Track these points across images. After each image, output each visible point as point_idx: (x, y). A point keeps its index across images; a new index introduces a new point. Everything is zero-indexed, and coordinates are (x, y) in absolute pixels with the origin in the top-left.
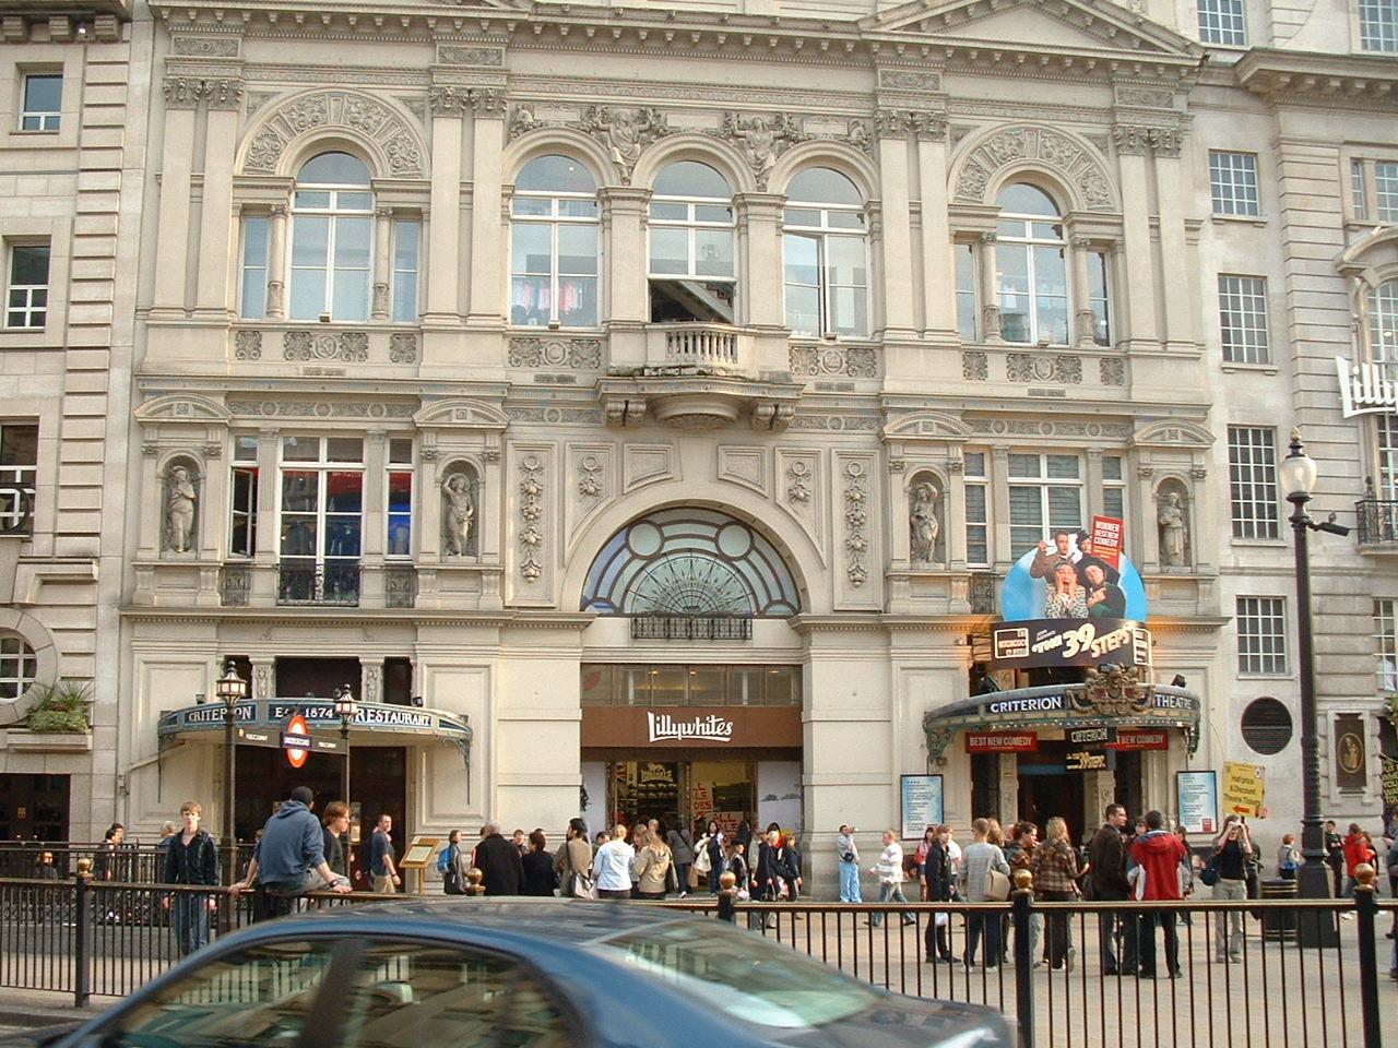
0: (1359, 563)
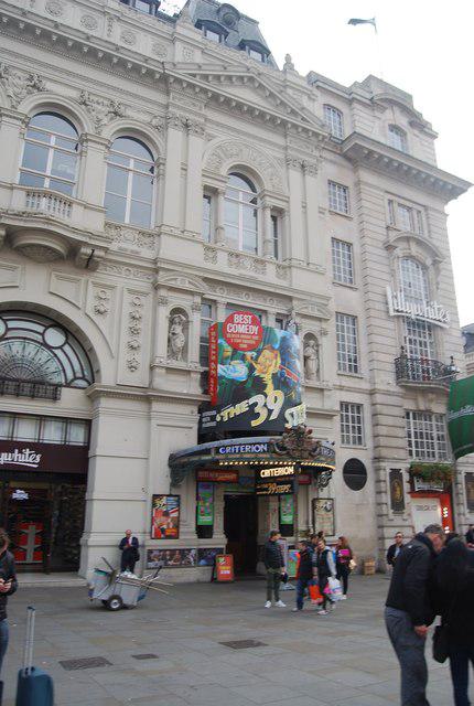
0: (394, 388)
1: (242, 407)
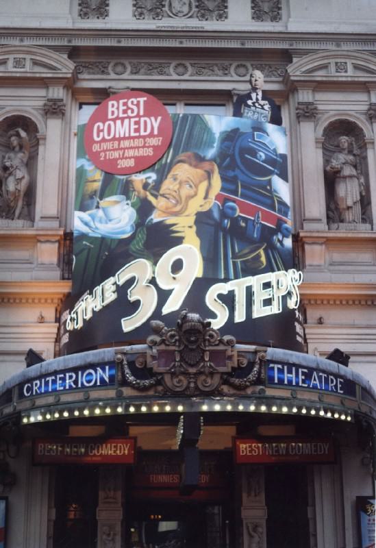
1: (107, 292)
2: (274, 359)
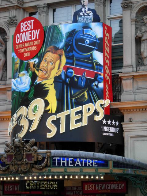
2: (55, 155)
